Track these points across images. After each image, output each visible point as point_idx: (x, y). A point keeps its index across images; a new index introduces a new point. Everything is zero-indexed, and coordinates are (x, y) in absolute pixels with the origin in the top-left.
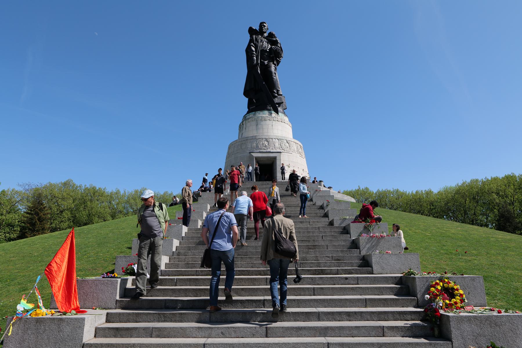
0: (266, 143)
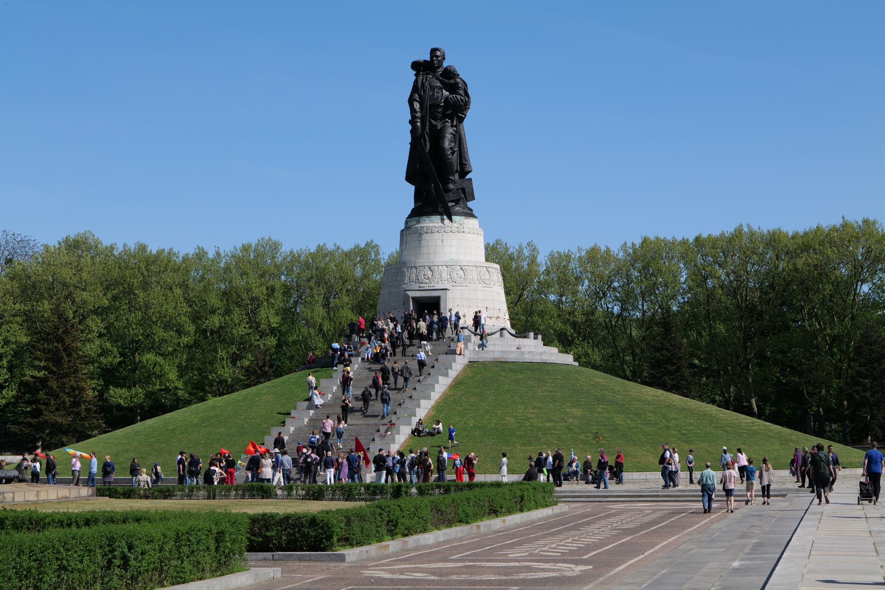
0: (429, 273)
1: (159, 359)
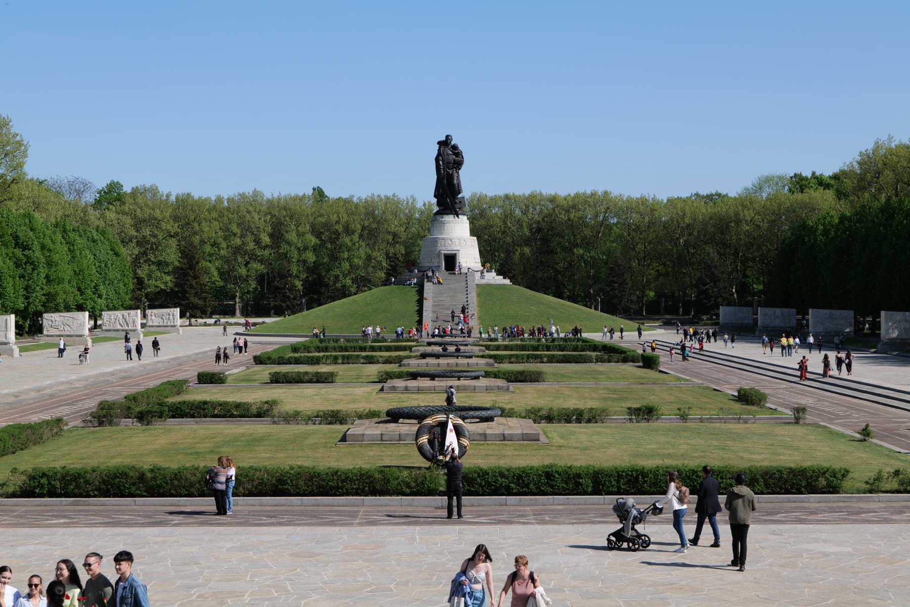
1: (208, 263)
